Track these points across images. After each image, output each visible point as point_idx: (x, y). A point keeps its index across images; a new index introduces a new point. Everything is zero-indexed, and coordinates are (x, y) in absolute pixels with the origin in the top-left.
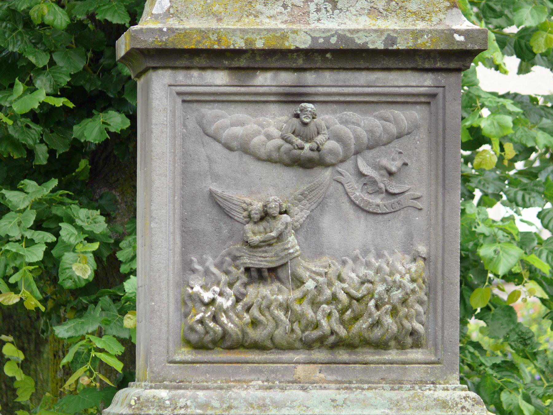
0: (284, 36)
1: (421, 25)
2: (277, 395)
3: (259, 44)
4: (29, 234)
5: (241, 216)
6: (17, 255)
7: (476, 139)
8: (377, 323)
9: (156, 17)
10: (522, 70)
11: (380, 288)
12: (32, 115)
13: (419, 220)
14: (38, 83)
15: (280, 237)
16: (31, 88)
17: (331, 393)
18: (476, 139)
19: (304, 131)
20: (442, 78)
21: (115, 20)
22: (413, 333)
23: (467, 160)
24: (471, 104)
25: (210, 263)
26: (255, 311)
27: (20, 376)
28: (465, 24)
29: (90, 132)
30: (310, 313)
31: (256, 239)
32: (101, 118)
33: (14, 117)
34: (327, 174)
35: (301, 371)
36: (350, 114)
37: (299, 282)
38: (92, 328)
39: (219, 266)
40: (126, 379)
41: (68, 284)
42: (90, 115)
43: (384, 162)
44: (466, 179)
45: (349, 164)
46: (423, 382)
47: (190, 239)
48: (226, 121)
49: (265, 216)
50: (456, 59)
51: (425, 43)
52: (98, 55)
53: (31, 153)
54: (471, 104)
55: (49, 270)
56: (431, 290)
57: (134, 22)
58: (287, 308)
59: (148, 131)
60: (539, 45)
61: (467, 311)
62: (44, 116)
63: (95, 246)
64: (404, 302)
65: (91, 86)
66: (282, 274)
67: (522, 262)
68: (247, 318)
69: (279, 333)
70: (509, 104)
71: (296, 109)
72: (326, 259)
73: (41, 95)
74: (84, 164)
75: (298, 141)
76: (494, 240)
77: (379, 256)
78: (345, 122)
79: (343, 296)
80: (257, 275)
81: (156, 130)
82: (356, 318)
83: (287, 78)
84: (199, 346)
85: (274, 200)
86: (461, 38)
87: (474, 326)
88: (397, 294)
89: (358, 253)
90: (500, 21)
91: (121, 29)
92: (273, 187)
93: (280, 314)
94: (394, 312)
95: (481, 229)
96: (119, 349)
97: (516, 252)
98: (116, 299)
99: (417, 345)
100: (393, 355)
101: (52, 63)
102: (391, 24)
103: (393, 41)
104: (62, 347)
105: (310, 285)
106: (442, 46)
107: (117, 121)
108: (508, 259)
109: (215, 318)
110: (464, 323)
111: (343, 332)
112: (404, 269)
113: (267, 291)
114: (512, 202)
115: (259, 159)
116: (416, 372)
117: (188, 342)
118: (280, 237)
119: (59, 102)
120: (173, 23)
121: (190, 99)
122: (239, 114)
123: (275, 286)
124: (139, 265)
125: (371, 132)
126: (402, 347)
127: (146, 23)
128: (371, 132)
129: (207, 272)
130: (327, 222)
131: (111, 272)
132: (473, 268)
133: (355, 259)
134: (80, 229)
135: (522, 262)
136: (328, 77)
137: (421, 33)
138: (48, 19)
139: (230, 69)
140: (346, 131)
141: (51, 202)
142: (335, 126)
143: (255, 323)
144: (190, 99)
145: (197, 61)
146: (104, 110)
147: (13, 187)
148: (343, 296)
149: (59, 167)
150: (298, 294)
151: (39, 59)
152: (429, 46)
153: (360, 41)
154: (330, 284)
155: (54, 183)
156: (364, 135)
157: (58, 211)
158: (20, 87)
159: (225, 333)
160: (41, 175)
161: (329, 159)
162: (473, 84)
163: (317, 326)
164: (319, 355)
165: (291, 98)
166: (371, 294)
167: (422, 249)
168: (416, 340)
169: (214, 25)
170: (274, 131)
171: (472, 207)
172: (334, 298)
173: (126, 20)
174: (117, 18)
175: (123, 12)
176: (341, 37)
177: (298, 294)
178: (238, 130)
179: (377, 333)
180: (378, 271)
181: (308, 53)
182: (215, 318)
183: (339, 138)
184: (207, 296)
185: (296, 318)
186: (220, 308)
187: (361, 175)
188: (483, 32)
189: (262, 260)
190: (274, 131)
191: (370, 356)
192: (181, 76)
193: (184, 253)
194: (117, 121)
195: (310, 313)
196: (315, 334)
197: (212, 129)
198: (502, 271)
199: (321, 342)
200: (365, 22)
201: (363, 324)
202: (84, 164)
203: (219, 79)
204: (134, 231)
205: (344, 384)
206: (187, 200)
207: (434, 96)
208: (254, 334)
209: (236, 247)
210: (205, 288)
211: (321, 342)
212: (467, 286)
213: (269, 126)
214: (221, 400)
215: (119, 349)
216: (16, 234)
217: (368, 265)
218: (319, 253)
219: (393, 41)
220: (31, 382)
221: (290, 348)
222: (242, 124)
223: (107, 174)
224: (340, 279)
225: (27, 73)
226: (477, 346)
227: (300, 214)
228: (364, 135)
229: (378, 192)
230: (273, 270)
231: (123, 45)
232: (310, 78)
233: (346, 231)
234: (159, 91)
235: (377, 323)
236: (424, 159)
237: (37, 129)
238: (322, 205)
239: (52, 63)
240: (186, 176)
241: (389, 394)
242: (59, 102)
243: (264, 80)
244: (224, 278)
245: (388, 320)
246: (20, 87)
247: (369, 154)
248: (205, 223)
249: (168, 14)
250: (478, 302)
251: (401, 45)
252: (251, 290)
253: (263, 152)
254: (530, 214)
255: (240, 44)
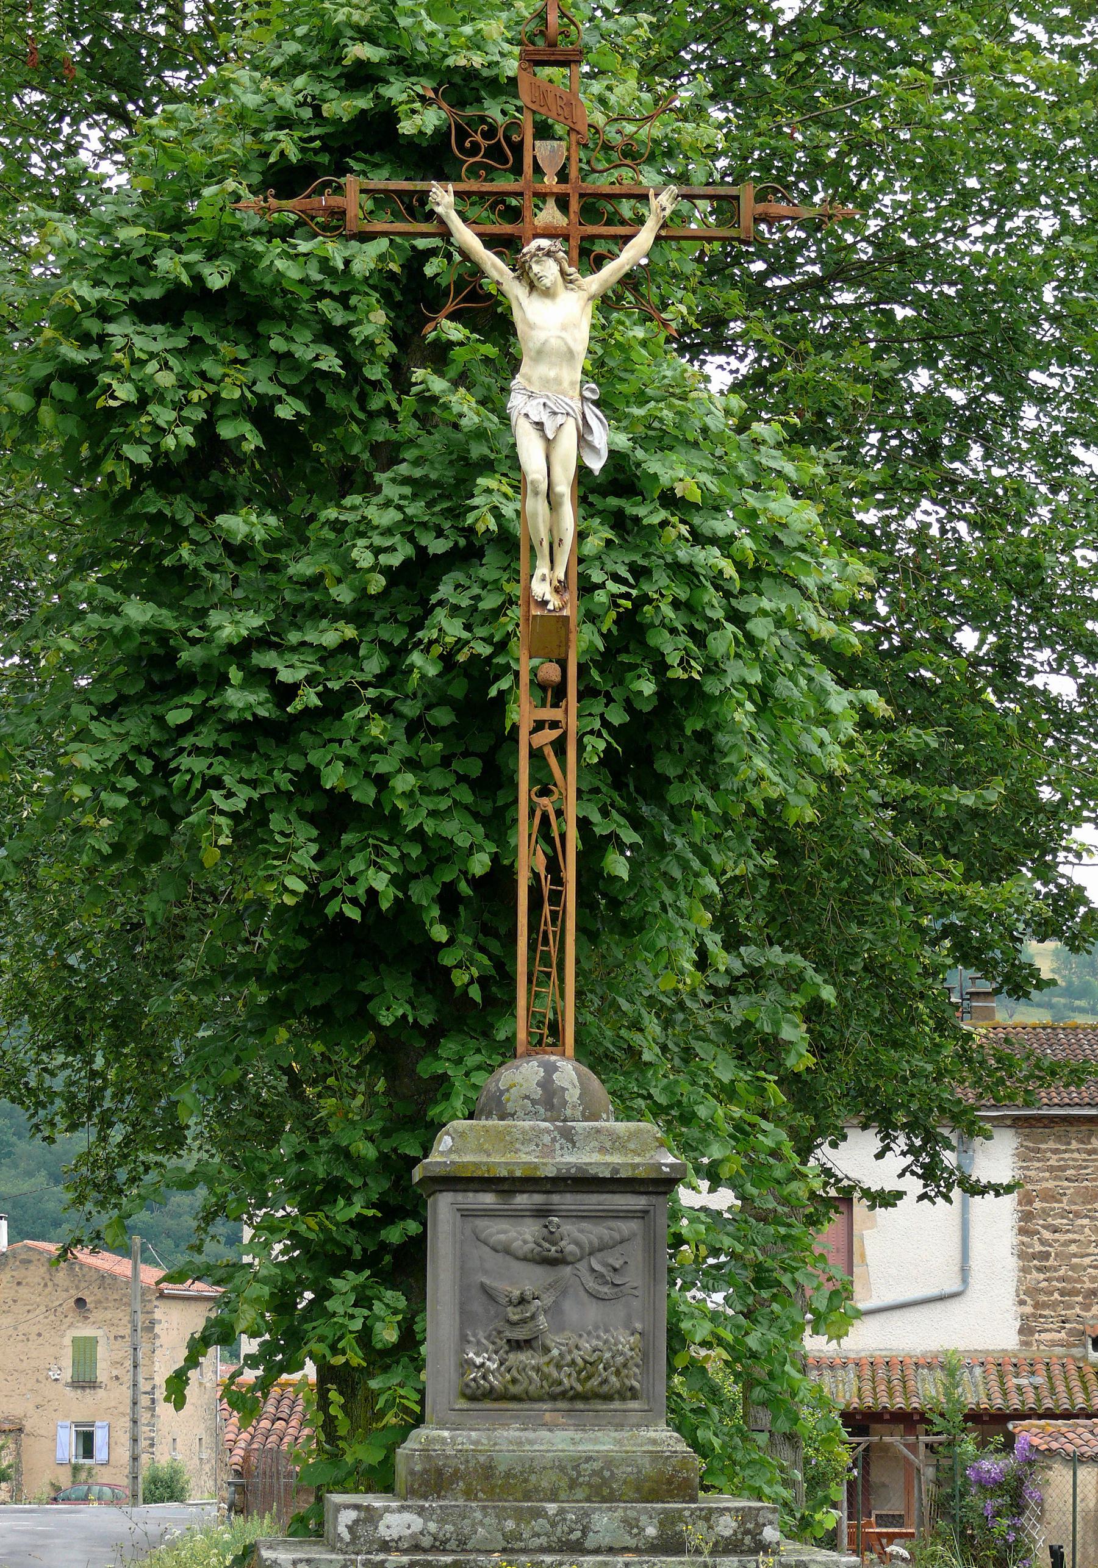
0: (536, 1167)
1: (637, 1160)
2: (531, 1435)
3: (518, 1174)
4: (350, 1311)
5: (504, 1301)
6: (343, 1326)
7: (678, 1240)
8: (605, 1381)
9: (442, 1153)
10: (711, 1190)
11: (607, 1355)
12: (351, 1223)
13: (636, 1303)
14: (355, 1199)
15: (533, 1317)
16: (349, 1203)
17: (570, 1434)
18: (678, 1240)
19: (551, 1238)
20: (653, 1199)
21: (412, 1154)
22: (632, 1388)
23: (671, 1256)
24: (675, 1215)
25: (481, 1335)
26: (514, 1372)
27: (341, 1415)
28: (671, 1160)
29: (394, 1235)
30: (555, 1374)
31: (516, 1318)
32: (401, 1225)
33: (337, 1224)
34: (568, 1270)
35: (548, 1416)
36: (585, 1225)
37: (547, 1350)
38: (396, 1381)
39: (488, 1338)
40: (419, 1420)
41: (379, 1346)
42: (393, 1223)
43: (611, 1261)
44: (671, 1270)
45: (584, 1262)
46: (638, 1426)
47: (466, 1318)
48: (493, 1230)
49: (522, 1301)
50: (663, 1185)
51: (640, 1173)
52: (399, 1178)
53: (350, 1250)
54: (675, 1215)
55: (365, 1337)
56: (645, 1356)
57: (426, 1156)
58: (538, 1370)
59: (435, 1237)
60: (725, 1172)
61: (672, 1370)
62: (359, 1223)
63: (400, 1317)
64: (625, 1365)
65: (394, 1200)
66: (534, 1344)
67: (713, 1333)
68: (508, 1377)
69: (532, 1388)
70: (702, 1215)
71: (546, 1221)
72: (567, 1333)
73: (358, 1208)
74: (387, 1258)
75: (546, 1245)
76: (692, 1316)
77: (607, 1331)
78: (581, 1231)
79: (579, 1361)
80: (517, 1345)
81: (441, 1237)
82: (589, 1378)
83: (538, 1198)
84: (472, 1398)
85: (529, 1289)
86: (666, 1169)
87: (677, 1379)
88: (620, 1359)
89: (592, 1330)
90: (696, 1154)
91: (416, 1161)
92: (529, 1280)
93: (533, 1374)
94: (618, 1373)
95: (683, 1308)
96: (417, 1397)
97: (708, 1326)
98: (413, 1360)
99: (635, 1397)
100: (616, 1405)
101: (365, 1184)
102: (616, 1159)
103: (617, 1171)
104: (374, 1395)
105: (555, 1352)
106: (653, 1175)
107: (413, 1227)
108: (703, 1330)
109: (484, 1377)
110: (669, 1377)
111: (579, 1388)
112: (625, 1341)
113: (524, 1357)
114: (705, 1288)
115: (518, 1258)
116: (634, 1418)
117: (464, 1395)
118: (533, 1317)
119: (370, 1213)
120: (455, 1157)
121: (466, 1214)
122: (503, 1225)
123: (530, 1353)
124: (428, 1334)
125: (601, 1239)
126: (623, 1398)
127: (434, 1158)
128: (601, 1239)
129: (479, 1343)
130: (568, 1305)
131: (410, 1339)
132: (676, 1339)
133: (589, 1333)
134: (387, 1305)
135: (713, 1333)
136: (569, 1198)
137: (638, 1165)
138: (363, 1152)
139: (496, 1191)
140: (582, 1238)
141: (364, 1286)
142: (574, 1234)
143: (514, 1381)
144: (466, 1214)
145: (471, 1186)
146: (403, 1219)
147: (337, 1276)
148: (579, 1361)
149: (369, 1261)
150: (546, 1359)
151: (356, 1182)
152: (644, 1175)
153: (592, 1171)
154: (570, 1352)
155: (367, 1273)
156: (596, 1241)
157: (369, 1293)
158: (341, 1202)
159: (492, 1388)
160: (358, 1268)
161: (570, 1258)
162: (676, 1201)
163: (560, 1383)
164: (562, 1405)
165: (541, 1213)
166: (600, 1359)
167: (638, 1326)
168: (633, 1394)
169: (485, 1159)
170: (528, 1237)
171: (675, 1292)
172: (573, 1363)
173: (420, 1154)
174: (413, 1152)
175: (418, 1147)
176: (579, 1168)
177: (546, 1359)
178: (502, 1237)
179: (605, 1388)
180: (606, 1342)
181: (554, 1180)
182: (484, 1377)
183: (577, 1243)
184: (478, 1361)
185: (545, 1377)
186: (488, 1370)
187: (593, 1270)
188: (684, 1165)
189: (520, 1334)
190: (528, 1237)
191: (600, 1406)
192: (460, 1197)
193: (462, 1329)
194: (413, 1227)
195: (555, 1374)
196: (559, 1389)
197: (483, 1236)
198: (697, 1340)
199: (563, 1395)
200: (596, 1158)
201: (595, 1382)
202: (387, 1258)
203: (488, 1199)
204: (424, 1309)
205: (580, 1427)
206: (464, 1289)
207: (646, 1212)
208: (514, 1389)
209: (500, 1324)
210: (477, 1354)
211: (563, 1395)
212: (672, 1352)
213: (525, 1234)
214: (489, 1439)
215: (417, 1397)
216: (341, 1310)
217: (598, 1338)
218: (560, 1329)
219: (617, 1171)
220: (347, 1422)
221: (540, 1399)
222: (505, 1232)
223: (407, 1267)
224: (577, 1348)
225: (348, 1193)
226: (679, 1395)
227: (548, 1300)
228: (596, 1241)
229: (606, 1283)
230: (527, 1342)
231: (417, 1174)
232: (556, 1198)
233: (581, 1312)
234: (444, 1207)
235: (605, 1381)
236: (640, 1258)
237: (354, 1233)
238: (564, 1293)
239: (365, 1184)
240: (464, 1271)
241: (613, 1434)
242: (370, 1213)
243: (522, 1200)
244: (491, 1347)
245: (613, 1379)
246: (341, 1202)
247: (599, 1255)
248: (478, 1305)
249: (450, 1151)
250: (680, 1362)
251: (623, 1175)
252: (511, 1356)
253: (520, 1253)
254: (718, 1297)
255: (504, 1173)
